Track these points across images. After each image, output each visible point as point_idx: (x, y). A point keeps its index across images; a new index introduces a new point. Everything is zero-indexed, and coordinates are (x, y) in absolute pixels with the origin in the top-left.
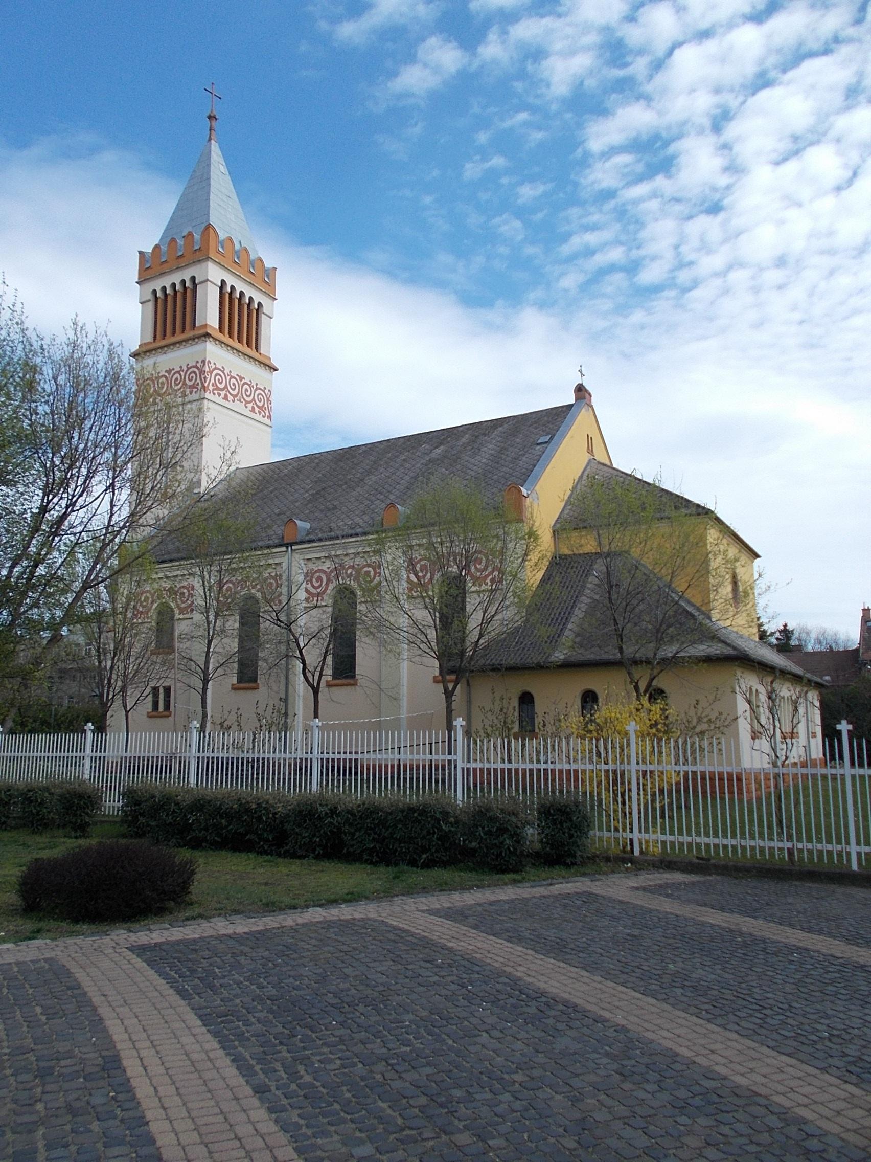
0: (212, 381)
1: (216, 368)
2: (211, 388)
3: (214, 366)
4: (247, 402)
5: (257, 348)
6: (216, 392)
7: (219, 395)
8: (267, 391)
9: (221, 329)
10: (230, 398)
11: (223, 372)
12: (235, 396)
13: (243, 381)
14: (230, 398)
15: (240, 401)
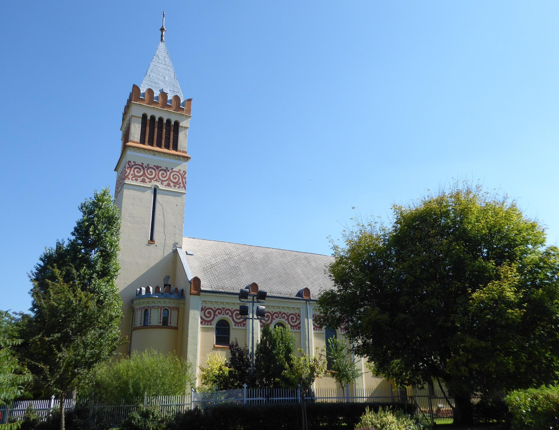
0: (132, 172)
1: (135, 165)
2: (130, 177)
3: (133, 164)
4: (162, 181)
5: (175, 148)
6: (134, 179)
7: (136, 180)
8: (181, 172)
9: (142, 141)
10: (147, 180)
11: (142, 166)
12: (151, 179)
13: (160, 169)
14: (147, 180)
15: (156, 180)
